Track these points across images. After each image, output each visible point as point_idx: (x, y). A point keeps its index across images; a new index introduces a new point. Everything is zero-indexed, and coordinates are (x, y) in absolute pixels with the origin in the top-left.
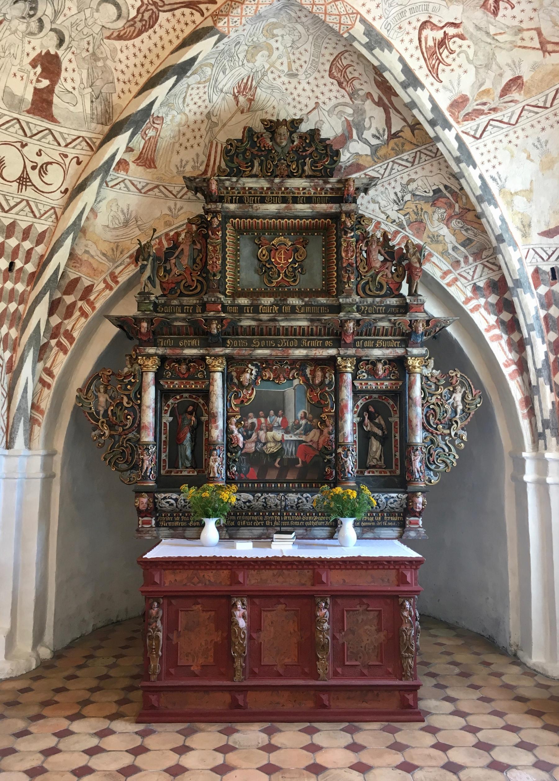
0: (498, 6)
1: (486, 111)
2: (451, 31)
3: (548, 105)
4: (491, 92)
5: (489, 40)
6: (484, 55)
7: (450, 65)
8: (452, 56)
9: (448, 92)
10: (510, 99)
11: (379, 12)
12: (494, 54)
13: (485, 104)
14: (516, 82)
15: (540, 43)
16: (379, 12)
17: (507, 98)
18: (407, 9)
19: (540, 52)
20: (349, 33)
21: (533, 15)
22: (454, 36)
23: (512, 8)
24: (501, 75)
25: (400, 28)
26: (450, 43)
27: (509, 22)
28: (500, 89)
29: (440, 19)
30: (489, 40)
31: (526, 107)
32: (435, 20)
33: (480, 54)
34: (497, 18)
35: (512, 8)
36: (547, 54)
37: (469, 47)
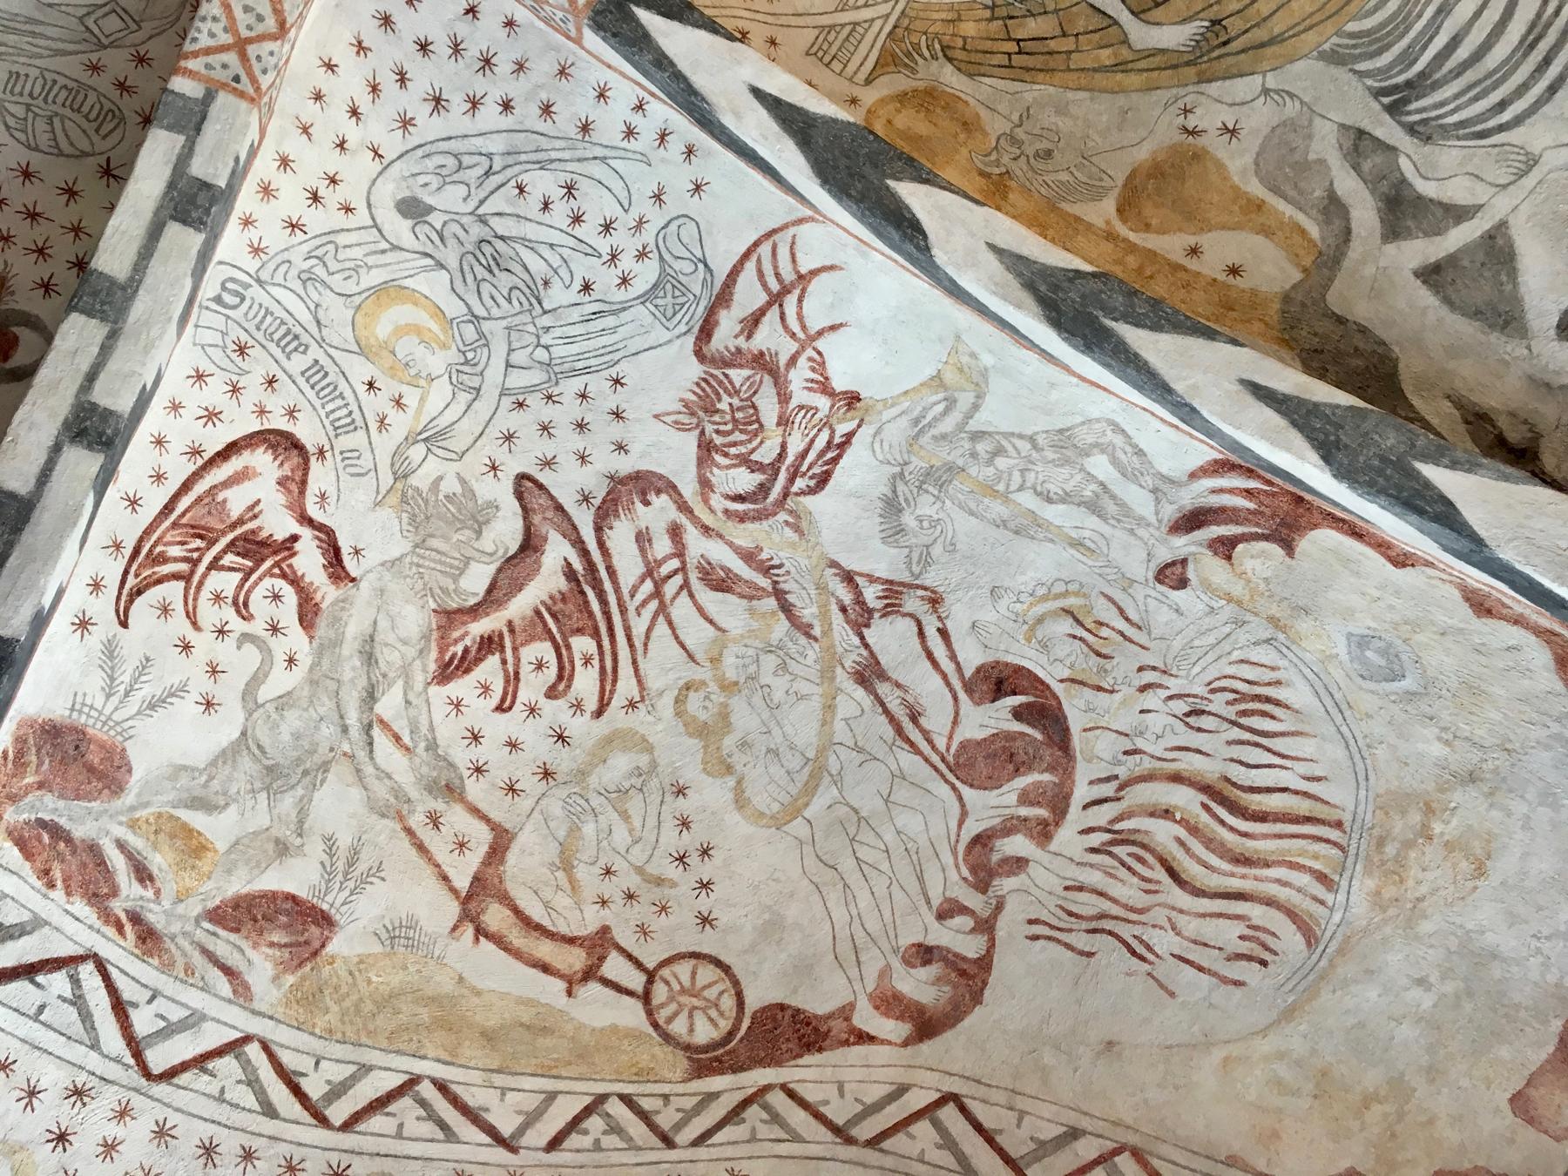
0: (478, 660)
1: (118, 906)
2: (309, 560)
3: (338, 1112)
4: (205, 865)
5: (353, 718)
6: (297, 736)
7: (195, 625)
8: (229, 613)
9: (97, 680)
10: (234, 960)
11: (274, 237)
12: (325, 767)
13: (143, 874)
14: (300, 923)
15: (476, 879)
16: (274, 237)
17: (224, 944)
18: (315, 352)
19: (453, 909)
20: (209, 97)
21: (530, 783)
22: (295, 581)
23: (500, 708)
24: (283, 849)
25: (242, 350)
26: (268, 582)
27: (449, 732)
28: (238, 885)
29: (332, 492)
30: (353, 718)
31: (253, 1051)
32: (320, 476)
33: (293, 720)
34: (434, 690)
35: (500, 708)
36: (469, 931)
37: (291, 661)
